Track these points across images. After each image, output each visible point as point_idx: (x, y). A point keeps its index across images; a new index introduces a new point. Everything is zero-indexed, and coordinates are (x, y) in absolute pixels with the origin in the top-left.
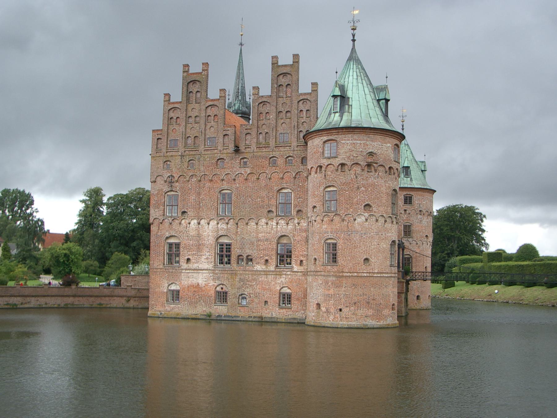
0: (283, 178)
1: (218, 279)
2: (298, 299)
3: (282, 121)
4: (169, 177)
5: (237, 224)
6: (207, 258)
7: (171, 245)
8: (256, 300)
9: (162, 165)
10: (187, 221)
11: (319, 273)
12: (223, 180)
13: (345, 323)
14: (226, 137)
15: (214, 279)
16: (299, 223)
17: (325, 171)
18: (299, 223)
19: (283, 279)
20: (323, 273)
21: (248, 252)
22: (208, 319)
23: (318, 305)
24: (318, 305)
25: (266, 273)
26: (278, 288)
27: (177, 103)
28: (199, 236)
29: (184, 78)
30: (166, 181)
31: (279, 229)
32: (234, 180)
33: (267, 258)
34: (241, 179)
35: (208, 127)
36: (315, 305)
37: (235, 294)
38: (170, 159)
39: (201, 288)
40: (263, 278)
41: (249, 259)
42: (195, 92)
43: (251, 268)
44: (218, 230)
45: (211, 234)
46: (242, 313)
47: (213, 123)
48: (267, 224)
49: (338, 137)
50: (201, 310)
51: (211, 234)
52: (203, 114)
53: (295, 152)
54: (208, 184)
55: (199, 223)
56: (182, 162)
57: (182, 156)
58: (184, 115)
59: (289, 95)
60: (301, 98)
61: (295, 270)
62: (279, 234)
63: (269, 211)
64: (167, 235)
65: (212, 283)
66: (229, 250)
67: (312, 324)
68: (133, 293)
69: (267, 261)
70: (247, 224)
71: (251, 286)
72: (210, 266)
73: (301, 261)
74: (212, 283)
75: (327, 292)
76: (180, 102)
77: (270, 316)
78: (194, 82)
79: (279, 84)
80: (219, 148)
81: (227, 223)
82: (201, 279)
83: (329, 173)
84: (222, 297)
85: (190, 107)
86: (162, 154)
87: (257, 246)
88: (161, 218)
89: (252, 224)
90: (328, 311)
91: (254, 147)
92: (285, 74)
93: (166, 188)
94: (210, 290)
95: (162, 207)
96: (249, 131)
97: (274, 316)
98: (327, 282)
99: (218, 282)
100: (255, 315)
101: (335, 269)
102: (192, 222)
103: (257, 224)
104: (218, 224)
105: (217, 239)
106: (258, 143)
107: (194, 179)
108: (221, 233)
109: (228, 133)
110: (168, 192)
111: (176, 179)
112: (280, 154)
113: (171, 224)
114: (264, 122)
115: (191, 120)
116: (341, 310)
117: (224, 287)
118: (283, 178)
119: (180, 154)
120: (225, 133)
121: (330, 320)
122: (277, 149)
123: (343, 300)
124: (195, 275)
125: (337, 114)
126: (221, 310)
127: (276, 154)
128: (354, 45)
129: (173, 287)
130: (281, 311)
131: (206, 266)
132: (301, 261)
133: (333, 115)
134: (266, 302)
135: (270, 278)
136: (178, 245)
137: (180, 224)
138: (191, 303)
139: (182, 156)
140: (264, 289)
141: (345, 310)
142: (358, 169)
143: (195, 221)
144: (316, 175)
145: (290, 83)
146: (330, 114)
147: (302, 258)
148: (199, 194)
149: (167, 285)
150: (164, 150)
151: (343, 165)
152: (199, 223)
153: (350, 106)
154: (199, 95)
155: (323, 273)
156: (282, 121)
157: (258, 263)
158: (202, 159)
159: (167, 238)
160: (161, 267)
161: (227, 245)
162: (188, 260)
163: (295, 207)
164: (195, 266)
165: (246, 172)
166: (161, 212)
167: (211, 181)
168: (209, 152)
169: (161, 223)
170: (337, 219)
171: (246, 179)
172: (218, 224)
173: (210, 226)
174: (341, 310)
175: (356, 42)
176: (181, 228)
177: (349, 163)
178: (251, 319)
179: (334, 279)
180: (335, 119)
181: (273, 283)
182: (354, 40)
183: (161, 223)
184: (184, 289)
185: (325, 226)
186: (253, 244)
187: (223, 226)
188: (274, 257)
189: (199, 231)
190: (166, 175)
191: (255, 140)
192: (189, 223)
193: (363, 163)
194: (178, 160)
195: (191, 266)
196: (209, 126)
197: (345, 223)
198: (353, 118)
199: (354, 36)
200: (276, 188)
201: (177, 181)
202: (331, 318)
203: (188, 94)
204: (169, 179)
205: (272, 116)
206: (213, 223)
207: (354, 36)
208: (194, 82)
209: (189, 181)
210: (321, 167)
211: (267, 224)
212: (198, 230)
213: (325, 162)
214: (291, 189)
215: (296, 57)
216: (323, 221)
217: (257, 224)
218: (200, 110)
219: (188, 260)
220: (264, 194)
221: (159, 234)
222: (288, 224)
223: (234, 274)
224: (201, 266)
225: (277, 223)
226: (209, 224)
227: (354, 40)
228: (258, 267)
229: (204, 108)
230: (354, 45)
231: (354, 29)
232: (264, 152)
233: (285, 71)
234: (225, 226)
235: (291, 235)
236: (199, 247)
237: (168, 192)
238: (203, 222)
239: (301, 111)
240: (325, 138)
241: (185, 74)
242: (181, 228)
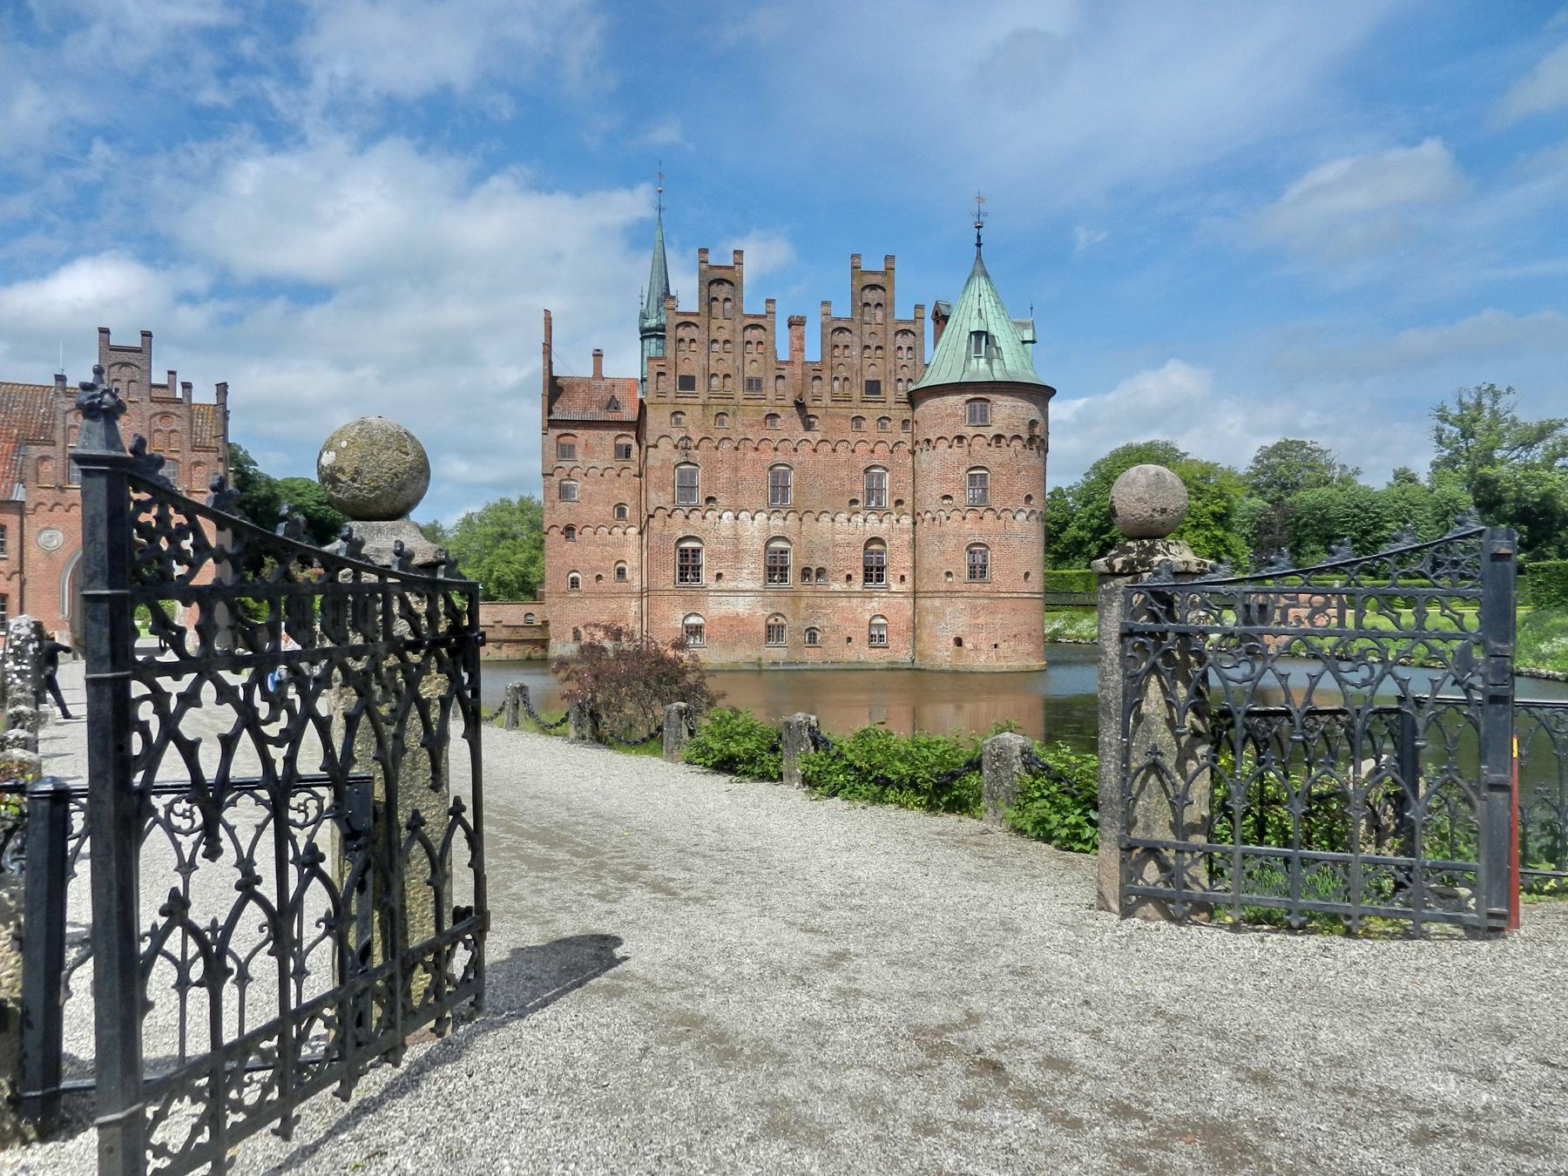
0: (872, 451)
1: (771, 605)
2: (898, 634)
3: (870, 361)
4: (682, 439)
5: (801, 519)
6: (752, 573)
7: (684, 554)
8: (834, 637)
9: (668, 418)
10: (717, 514)
12: (776, 449)
13: (1003, 665)
14: (780, 381)
15: (764, 606)
16: (898, 521)
17: (970, 445)
18: (898, 521)
19: (875, 605)
20: (966, 594)
21: (821, 563)
22: (758, 670)
23: (959, 642)
24: (959, 642)
25: (849, 595)
26: (868, 618)
27: (691, 314)
28: (737, 537)
29: (702, 273)
30: (676, 447)
31: (867, 528)
32: (796, 450)
33: (849, 572)
34: (808, 448)
35: (747, 361)
36: (951, 642)
37: (799, 628)
38: (682, 409)
39: (742, 620)
40: (844, 603)
41: (821, 572)
42: (721, 299)
43: (825, 588)
44: (769, 528)
45: (756, 534)
46: (812, 656)
47: (755, 355)
48: (849, 520)
49: (992, 397)
50: (742, 654)
51: (756, 534)
52: (739, 339)
53: (893, 412)
54: (751, 455)
55: (737, 518)
56: (704, 415)
57: (705, 406)
58: (705, 336)
59: (879, 321)
60: (902, 327)
61: (893, 589)
62: (869, 536)
63: (854, 502)
64: (681, 534)
65: (760, 612)
66: (784, 560)
67: (946, 666)
68: (505, 634)
69: (849, 577)
70: (817, 520)
71: (825, 615)
72: (758, 585)
73: (903, 578)
74: (760, 612)
75: (974, 621)
76: (698, 314)
77: (855, 659)
78: (720, 281)
79: (865, 301)
80: (769, 396)
81: (785, 519)
82: (740, 606)
83: (977, 448)
84: (773, 632)
85: (714, 324)
86: (667, 400)
87: (834, 553)
88: (670, 507)
89: (826, 519)
90: (976, 648)
91: (827, 400)
92: (873, 287)
93: (677, 457)
94: (757, 624)
95: (670, 489)
96: (818, 373)
97: (862, 658)
99: (770, 611)
100: (833, 659)
101: (987, 587)
102: (725, 516)
103: (833, 520)
104: (769, 519)
105: (768, 542)
106: (832, 393)
107: (726, 444)
108: (774, 533)
109: (782, 373)
110: (680, 464)
111: (696, 443)
112: (871, 412)
113: (687, 517)
114: (841, 360)
115: (716, 347)
116: (996, 646)
117: (779, 618)
118: (872, 451)
119: (700, 401)
120: (779, 373)
121: (982, 660)
122: (864, 405)
123: (999, 632)
124: (731, 599)
125: (982, 361)
126: (776, 653)
127: (864, 413)
128: (979, 253)
129: (692, 620)
130: (873, 651)
131: (749, 585)
132: (903, 578)
133: (974, 361)
134: (849, 639)
135: (854, 600)
136: (696, 551)
137: (704, 517)
138: (725, 645)
139: (705, 406)
140: (846, 619)
141: (1002, 646)
142: (1017, 444)
143: (730, 514)
145: (882, 301)
146: (968, 359)
147: (903, 573)
148: (736, 469)
149: (682, 617)
150: (672, 394)
151: (998, 437)
152: (737, 518)
153: (998, 349)
154: (728, 305)
155: (966, 594)
156: (870, 361)
157: (835, 580)
158: (740, 412)
159: (681, 540)
160: (671, 587)
161: (782, 552)
162: (719, 576)
163: (893, 494)
164: (731, 585)
165: (814, 438)
166: (670, 498)
167: (756, 449)
168: (752, 402)
169: (669, 516)
170: (989, 515)
171: (815, 450)
172: (769, 519)
173: (756, 522)
174: (996, 646)
176: (706, 525)
177: (1008, 435)
178: (826, 666)
179: (986, 601)
180: (981, 367)
181: (860, 610)
182: (979, 245)
183: (669, 516)
184: (712, 621)
186: (827, 550)
187: (777, 521)
188: (861, 571)
189: (736, 530)
190: (677, 435)
191: (829, 388)
192: (720, 517)
193: (1026, 436)
194: (698, 410)
195: (723, 585)
196: (748, 358)
197: (1002, 522)
198: (1008, 367)
199: (979, 237)
200: (863, 466)
201: (697, 447)
202: (983, 658)
203: (709, 301)
204: (682, 443)
205: (856, 352)
206: (761, 517)
207: (979, 237)
208: (720, 281)
209: (717, 448)
210: (960, 438)
211: (849, 520)
212: (735, 528)
213: (970, 431)
214: (885, 468)
215: (889, 259)
216: (964, 518)
217: (833, 520)
218: (734, 330)
219: (719, 576)
220: (844, 473)
221: (666, 533)
222: (881, 521)
223: (797, 597)
224: (741, 586)
225: (865, 520)
226: (753, 519)
227: (979, 245)
228: (836, 586)
229: (740, 328)
230: (979, 253)
231: (979, 227)
232: (843, 409)
233: (874, 282)
234: (780, 522)
235: (885, 538)
236: (737, 555)
237: (680, 464)
238: (742, 515)
239: (900, 348)
240: (971, 396)
241: (704, 266)
242: (706, 525)
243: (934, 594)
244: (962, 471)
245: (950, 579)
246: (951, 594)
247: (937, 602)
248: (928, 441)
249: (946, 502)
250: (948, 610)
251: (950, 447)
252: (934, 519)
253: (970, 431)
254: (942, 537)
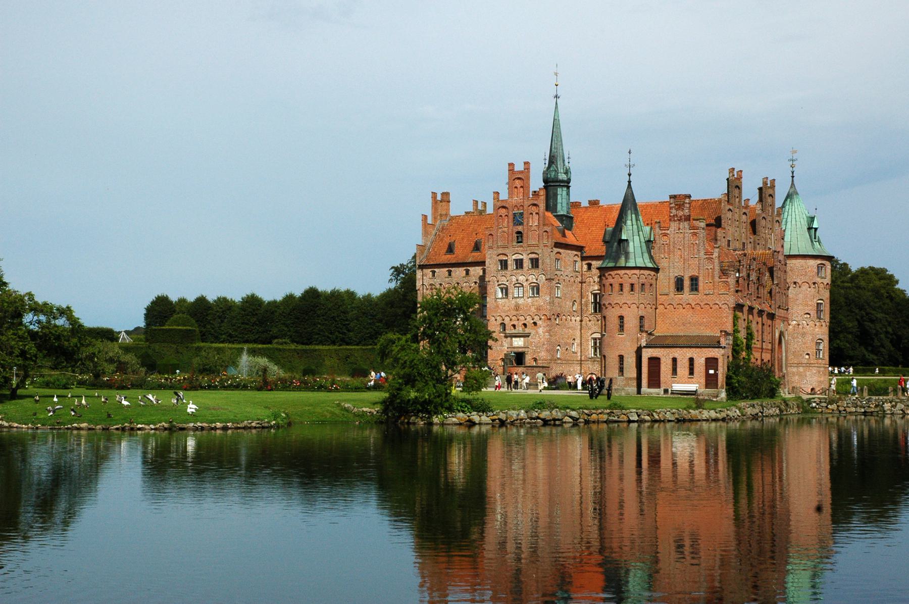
11: (814, 365)
20: (816, 365)
75: (820, 379)
98: (819, 372)
128: (793, 181)
144: (809, 289)
146: (812, 241)
155: (816, 365)
175: (794, 178)
182: (793, 177)
185: (817, 330)
199: (793, 173)
207: (793, 173)
210: (814, 283)
216: (815, 325)
227: (793, 177)
230: (793, 181)
243: (799, 365)
244: (815, 300)
245: (807, 357)
246: (809, 365)
247: (801, 369)
248: (795, 283)
249: (805, 316)
250: (808, 373)
251: (810, 287)
252: (799, 325)
253: (818, 280)
254: (804, 335)
